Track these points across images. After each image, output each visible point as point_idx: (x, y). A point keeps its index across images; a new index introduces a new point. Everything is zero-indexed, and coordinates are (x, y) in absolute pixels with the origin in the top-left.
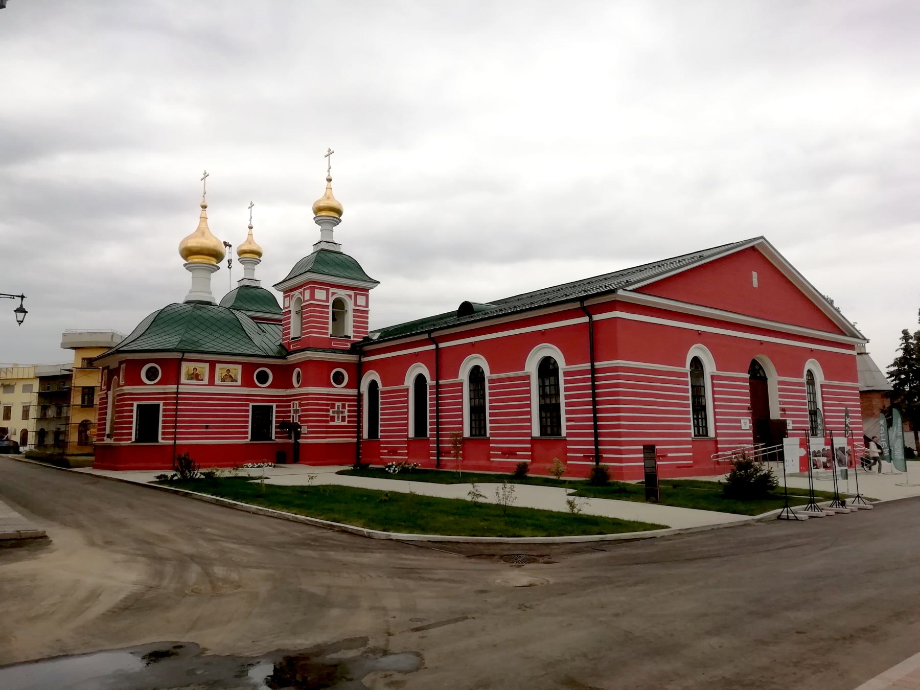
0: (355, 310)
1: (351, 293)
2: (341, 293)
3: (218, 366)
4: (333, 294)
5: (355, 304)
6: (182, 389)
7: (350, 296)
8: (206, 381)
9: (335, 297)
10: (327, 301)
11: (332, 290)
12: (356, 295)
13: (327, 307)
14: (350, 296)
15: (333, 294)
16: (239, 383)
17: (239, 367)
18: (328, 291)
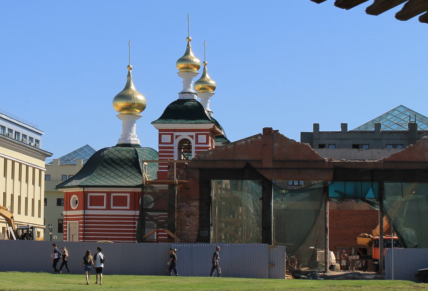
0: (196, 148)
1: (194, 134)
2: (185, 135)
3: (113, 195)
4: (177, 137)
5: (197, 143)
6: (88, 212)
7: (192, 137)
8: (104, 207)
9: (179, 139)
10: (172, 143)
11: (176, 134)
12: (197, 135)
13: (172, 148)
14: (192, 137)
15: (177, 137)
16: (128, 207)
17: (128, 195)
18: (172, 135)
